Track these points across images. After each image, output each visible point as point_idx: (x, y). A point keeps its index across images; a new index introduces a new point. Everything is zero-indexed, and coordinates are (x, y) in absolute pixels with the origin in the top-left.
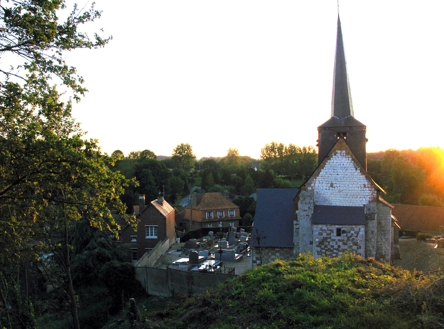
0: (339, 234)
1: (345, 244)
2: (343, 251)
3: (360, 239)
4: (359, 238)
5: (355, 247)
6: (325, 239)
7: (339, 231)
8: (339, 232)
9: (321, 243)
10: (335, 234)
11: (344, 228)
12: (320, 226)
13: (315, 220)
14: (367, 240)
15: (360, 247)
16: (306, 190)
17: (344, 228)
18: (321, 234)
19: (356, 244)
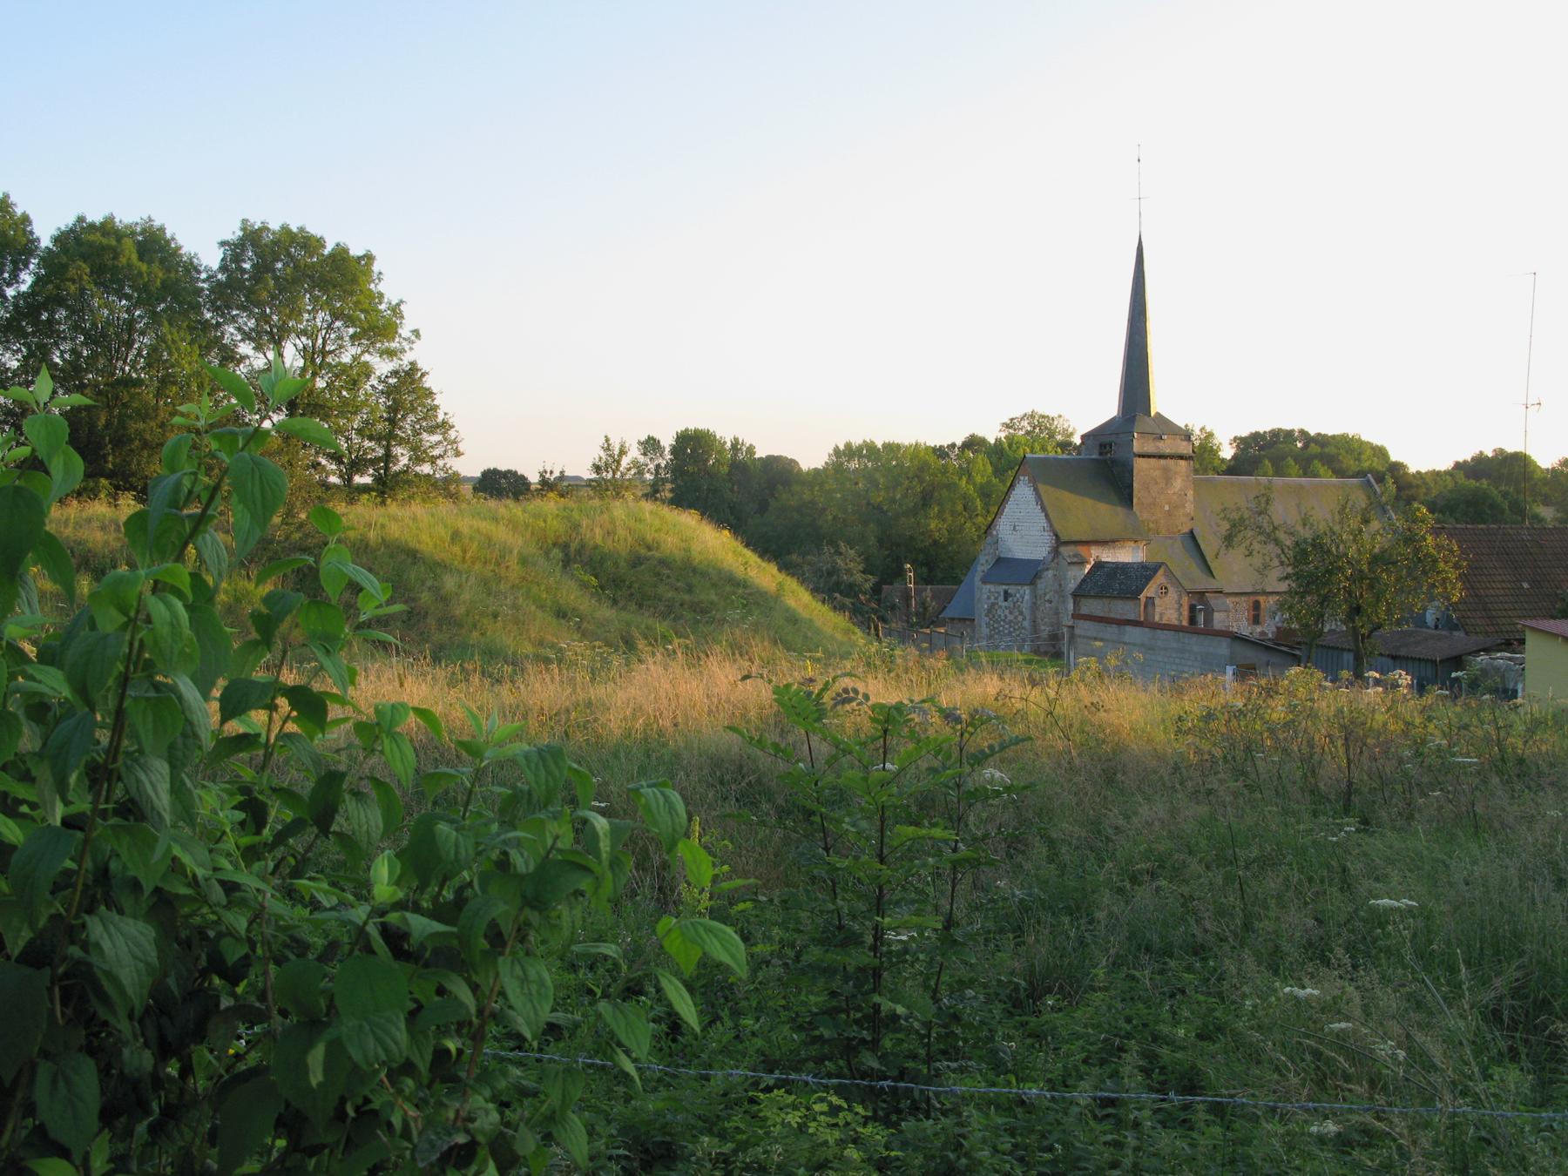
0: (1006, 600)
1: (1011, 613)
2: (1011, 621)
3: (1025, 607)
4: (1024, 605)
5: (1020, 618)
6: (993, 604)
7: (1006, 592)
8: (1007, 595)
9: (989, 610)
10: (1002, 598)
11: (1011, 590)
12: (988, 586)
13: (985, 581)
14: (1034, 607)
15: (1024, 619)
16: (991, 534)
17: (1011, 590)
18: (989, 598)
19: (1021, 613)
